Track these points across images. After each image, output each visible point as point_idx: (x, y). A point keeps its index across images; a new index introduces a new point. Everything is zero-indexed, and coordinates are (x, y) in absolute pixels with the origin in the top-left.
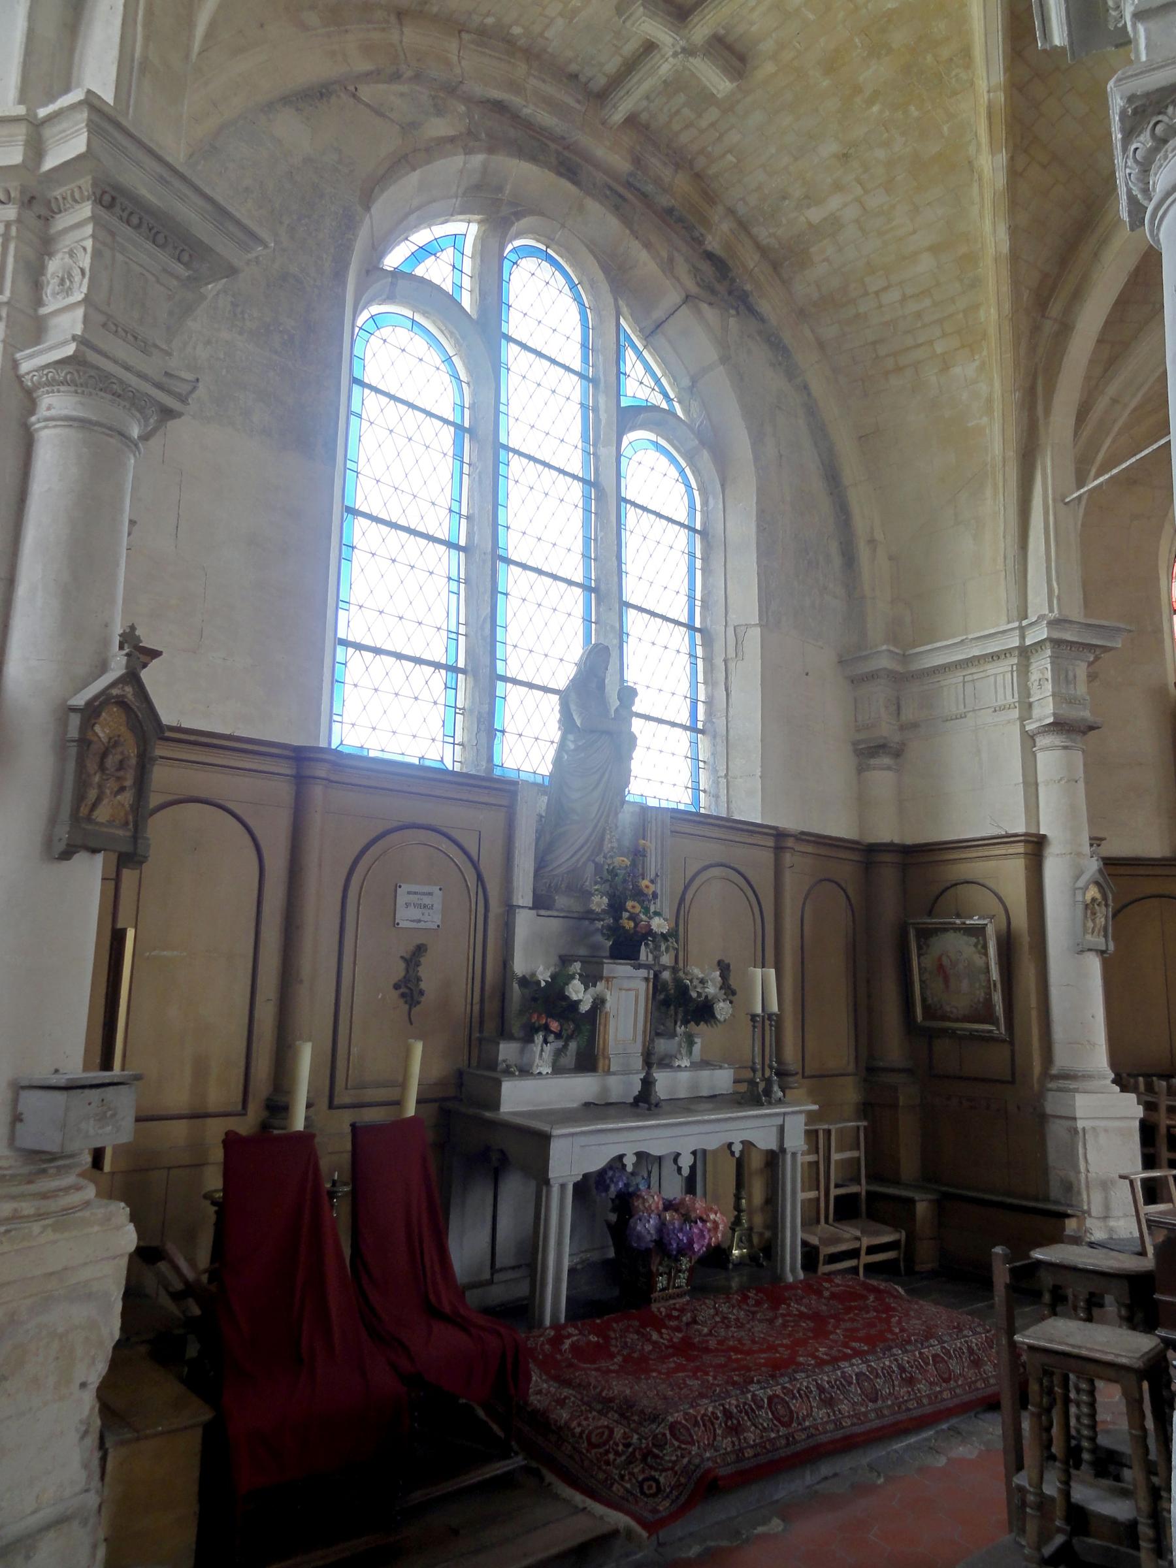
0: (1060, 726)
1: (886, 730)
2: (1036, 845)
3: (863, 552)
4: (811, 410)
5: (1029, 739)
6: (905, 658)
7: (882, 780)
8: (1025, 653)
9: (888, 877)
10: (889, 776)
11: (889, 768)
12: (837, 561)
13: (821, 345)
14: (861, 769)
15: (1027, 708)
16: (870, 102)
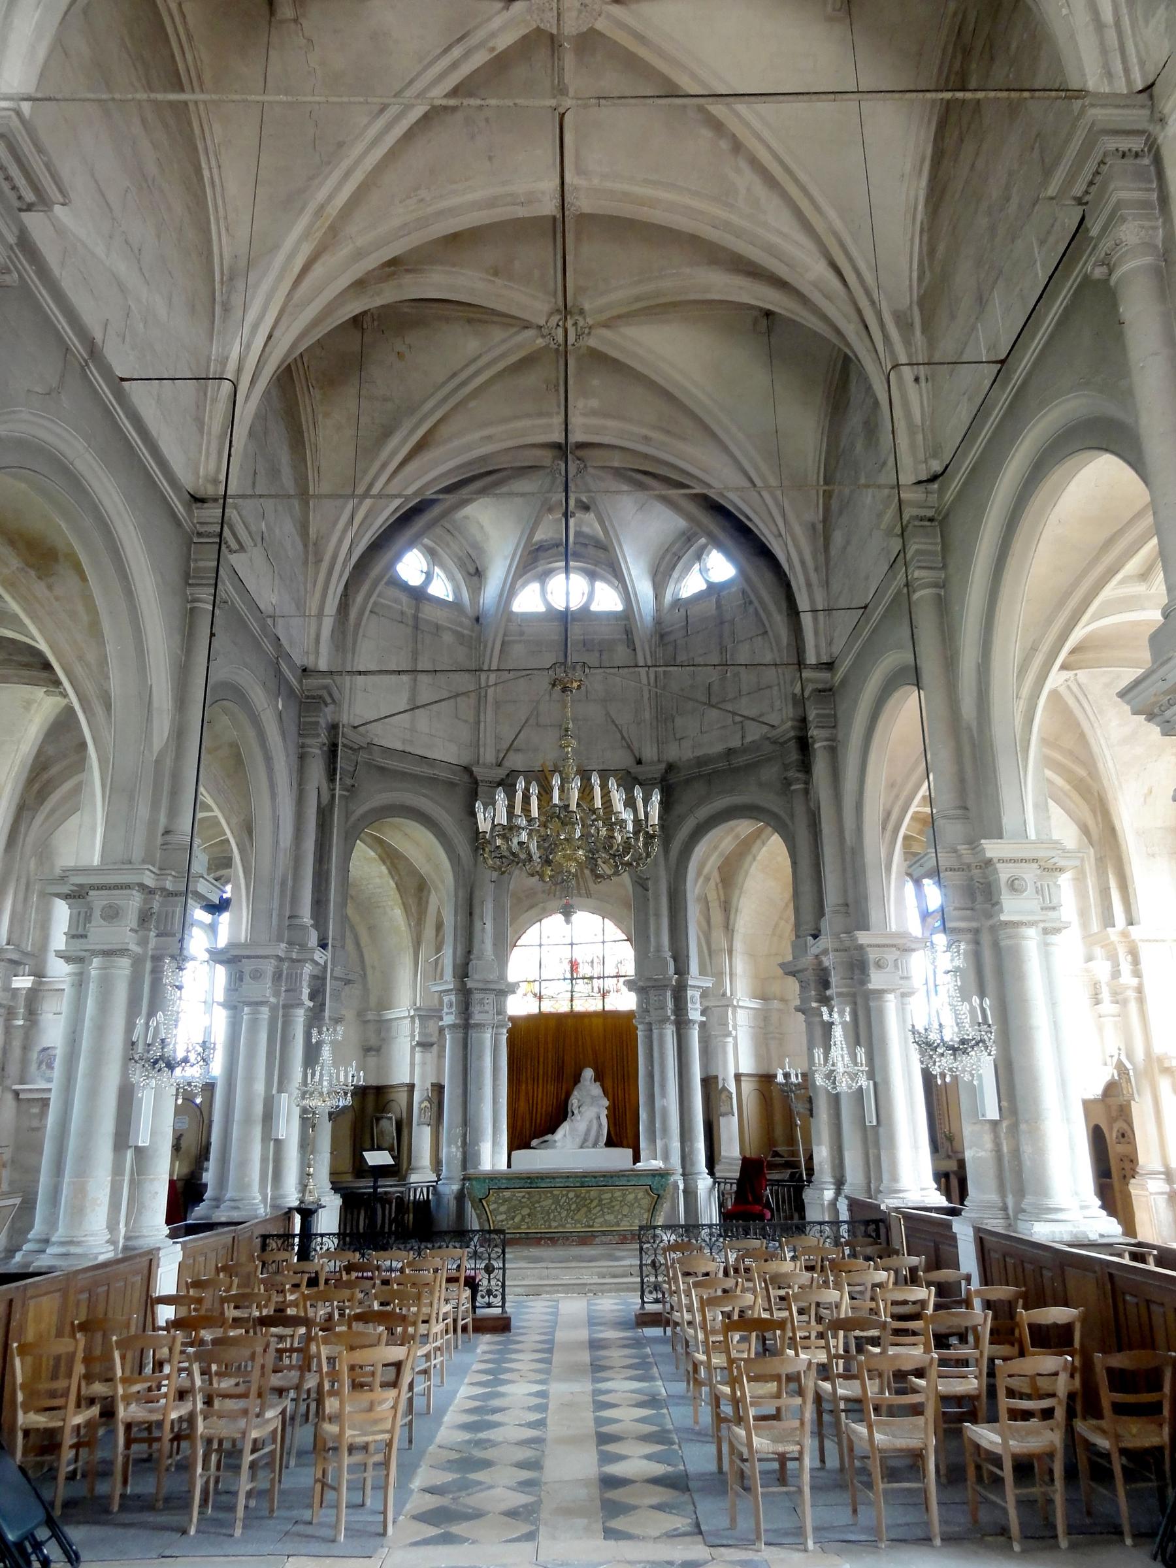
0: (419, 1044)
1: (373, 1042)
2: (411, 1087)
3: (369, 971)
5: (413, 1048)
6: (380, 1015)
7: (372, 1061)
9: (371, 1099)
10: (375, 1059)
15: (413, 1037)
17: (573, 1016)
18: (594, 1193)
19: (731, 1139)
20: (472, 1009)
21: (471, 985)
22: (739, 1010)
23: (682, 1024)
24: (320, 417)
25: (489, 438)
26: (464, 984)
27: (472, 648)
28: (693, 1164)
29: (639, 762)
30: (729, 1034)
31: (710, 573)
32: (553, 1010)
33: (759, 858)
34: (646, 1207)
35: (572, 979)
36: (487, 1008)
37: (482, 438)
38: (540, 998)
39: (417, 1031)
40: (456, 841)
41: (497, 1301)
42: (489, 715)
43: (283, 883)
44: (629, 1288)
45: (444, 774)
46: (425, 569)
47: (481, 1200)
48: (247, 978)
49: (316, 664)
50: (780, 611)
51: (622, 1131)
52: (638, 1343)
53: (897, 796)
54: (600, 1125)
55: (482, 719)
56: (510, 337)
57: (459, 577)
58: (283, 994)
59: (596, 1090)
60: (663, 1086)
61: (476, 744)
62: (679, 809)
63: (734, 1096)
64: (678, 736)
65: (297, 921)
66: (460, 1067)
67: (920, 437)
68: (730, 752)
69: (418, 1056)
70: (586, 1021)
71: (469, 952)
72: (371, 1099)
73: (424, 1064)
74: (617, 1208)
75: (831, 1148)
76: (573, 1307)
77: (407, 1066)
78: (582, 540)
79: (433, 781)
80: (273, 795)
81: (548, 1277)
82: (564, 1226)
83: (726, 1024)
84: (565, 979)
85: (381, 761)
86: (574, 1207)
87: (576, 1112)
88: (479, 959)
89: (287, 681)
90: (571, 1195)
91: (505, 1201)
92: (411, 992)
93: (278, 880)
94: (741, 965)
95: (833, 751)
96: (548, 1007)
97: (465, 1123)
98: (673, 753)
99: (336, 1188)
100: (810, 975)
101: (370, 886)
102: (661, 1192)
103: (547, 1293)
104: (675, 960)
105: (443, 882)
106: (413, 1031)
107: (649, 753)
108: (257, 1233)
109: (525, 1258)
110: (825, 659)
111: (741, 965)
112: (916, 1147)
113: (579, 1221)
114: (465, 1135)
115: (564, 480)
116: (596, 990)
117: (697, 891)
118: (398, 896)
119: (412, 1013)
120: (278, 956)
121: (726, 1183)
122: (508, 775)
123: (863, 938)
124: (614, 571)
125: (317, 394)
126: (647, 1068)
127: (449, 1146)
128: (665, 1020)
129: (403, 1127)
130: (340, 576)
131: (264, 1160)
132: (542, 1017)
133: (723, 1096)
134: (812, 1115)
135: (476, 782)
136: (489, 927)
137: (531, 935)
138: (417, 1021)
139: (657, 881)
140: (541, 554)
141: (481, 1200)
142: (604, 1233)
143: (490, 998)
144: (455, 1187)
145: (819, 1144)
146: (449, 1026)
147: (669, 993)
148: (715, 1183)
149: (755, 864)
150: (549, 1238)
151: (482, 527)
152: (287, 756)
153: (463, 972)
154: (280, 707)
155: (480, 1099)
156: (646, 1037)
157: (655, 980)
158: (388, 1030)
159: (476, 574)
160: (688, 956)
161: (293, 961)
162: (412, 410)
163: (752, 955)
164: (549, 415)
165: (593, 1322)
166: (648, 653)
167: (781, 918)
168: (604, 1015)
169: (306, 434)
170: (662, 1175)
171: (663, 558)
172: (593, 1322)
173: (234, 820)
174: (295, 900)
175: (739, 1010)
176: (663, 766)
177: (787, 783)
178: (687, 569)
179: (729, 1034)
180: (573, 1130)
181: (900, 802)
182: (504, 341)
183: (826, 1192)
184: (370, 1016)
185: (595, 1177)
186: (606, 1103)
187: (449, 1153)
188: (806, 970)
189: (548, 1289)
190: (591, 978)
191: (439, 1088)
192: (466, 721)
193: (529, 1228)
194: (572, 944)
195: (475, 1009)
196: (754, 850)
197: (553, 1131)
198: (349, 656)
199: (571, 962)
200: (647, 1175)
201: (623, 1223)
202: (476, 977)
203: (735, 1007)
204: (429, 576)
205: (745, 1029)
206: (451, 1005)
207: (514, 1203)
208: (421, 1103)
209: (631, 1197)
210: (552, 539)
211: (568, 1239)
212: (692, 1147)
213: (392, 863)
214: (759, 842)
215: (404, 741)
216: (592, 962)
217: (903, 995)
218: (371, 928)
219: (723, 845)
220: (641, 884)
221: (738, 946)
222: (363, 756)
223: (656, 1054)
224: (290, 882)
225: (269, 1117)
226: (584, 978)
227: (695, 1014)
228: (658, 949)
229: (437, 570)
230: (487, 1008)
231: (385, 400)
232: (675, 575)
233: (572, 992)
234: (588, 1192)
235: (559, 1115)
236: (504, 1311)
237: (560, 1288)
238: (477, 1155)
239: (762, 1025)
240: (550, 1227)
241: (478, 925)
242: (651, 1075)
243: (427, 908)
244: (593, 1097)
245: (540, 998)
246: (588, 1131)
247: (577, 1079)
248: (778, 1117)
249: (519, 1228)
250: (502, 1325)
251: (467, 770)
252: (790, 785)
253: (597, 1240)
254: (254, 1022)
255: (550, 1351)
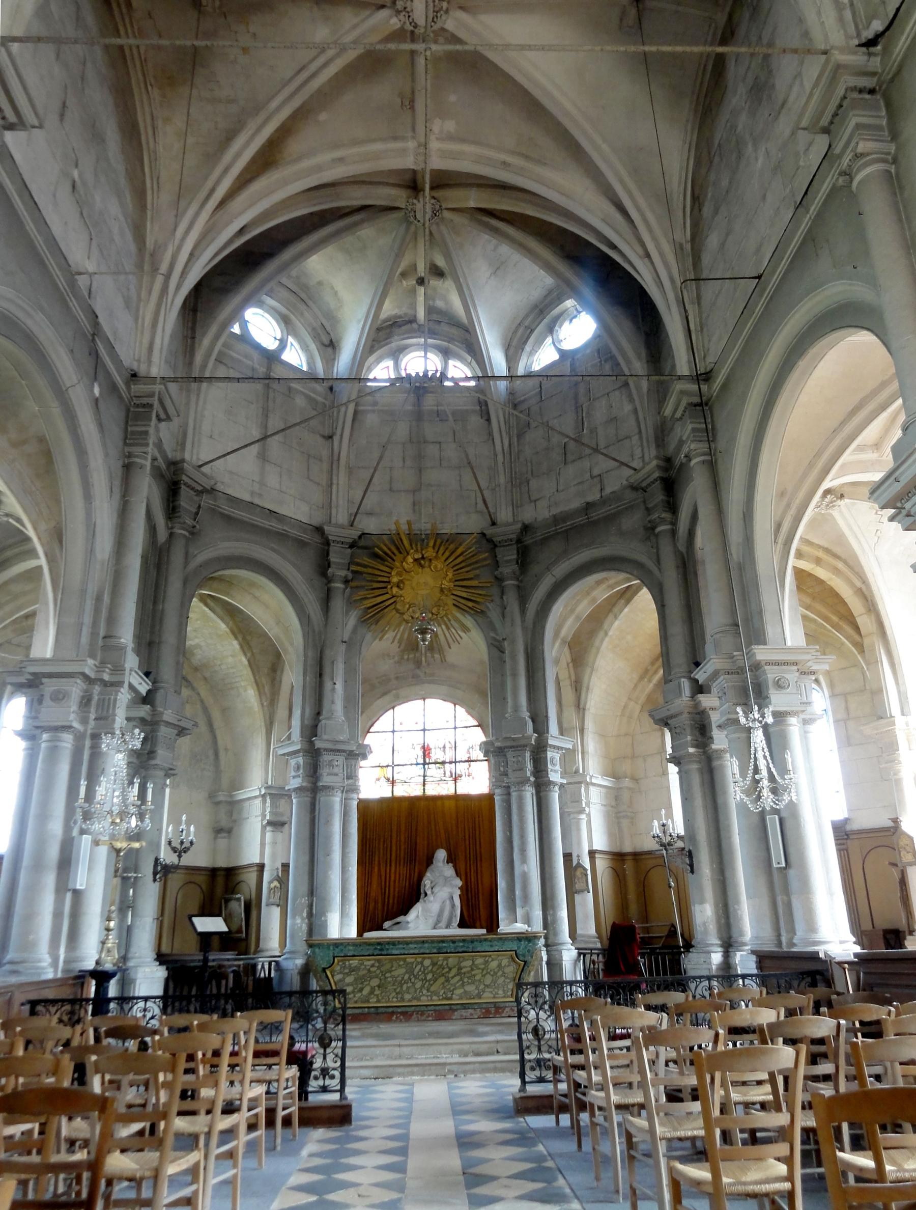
0: (270, 823)
1: (224, 823)
2: (261, 867)
3: (222, 753)
4: (202, 701)
5: (264, 828)
6: (231, 796)
7: (222, 842)
8: (264, 796)
9: (220, 881)
10: (225, 841)
11: (224, 838)
12: (212, 757)
13: (205, 679)
14: (215, 838)
15: (264, 816)
16: (197, 620)
17: (425, 799)
18: (452, 960)
19: (586, 917)
20: (320, 771)
21: (322, 755)
22: (591, 788)
23: (542, 785)
24: (160, 123)
25: (341, 160)
26: (312, 743)
27: (324, 408)
28: (556, 934)
29: (494, 524)
30: (582, 811)
31: (562, 344)
32: (406, 794)
33: (610, 633)
34: (511, 975)
35: (424, 764)
36: (336, 770)
37: (333, 160)
38: (393, 782)
39: (268, 810)
40: (306, 600)
41: (334, 1083)
42: (342, 478)
43: (99, 599)
44: (498, 1068)
45: (294, 532)
46: (279, 337)
47: (324, 970)
48: (47, 701)
49: (149, 372)
50: (639, 358)
51: (479, 907)
52: (523, 1138)
53: (788, 506)
54: (453, 906)
55: (335, 481)
56: (363, 21)
57: (313, 347)
58: (92, 723)
59: (449, 871)
60: (523, 851)
61: (328, 505)
62: (535, 569)
63: (589, 872)
64: (533, 498)
65: (112, 642)
66: (307, 834)
67: (848, 14)
68: (589, 506)
69: (268, 835)
70: (439, 803)
71: (319, 714)
72: (220, 881)
73: (274, 843)
74: (478, 977)
75: (716, 906)
76: (431, 1091)
77: (258, 845)
78: (435, 317)
79: (282, 537)
80: (88, 497)
81: (400, 1057)
82: (419, 1000)
83: (579, 801)
84: (417, 764)
85: (227, 509)
86: (429, 976)
87: (429, 892)
88: (328, 719)
89: (108, 374)
90: (427, 962)
91: (352, 970)
92: (264, 770)
93: (92, 589)
94: (592, 744)
95: (712, 466)
96: (401, 791)
97: (311, 892)
98: (528, 515)
99: (161, 958)
100: (685, 720)
101: (223, 667)
102: (528, 958)
103: (399, 1075)
104: (533, 721)
105: (292, 644)
106: (264, 810)
107: (504, 515)
108: (20, 997)
109: (377, 1036)
110: (701, 370)
111: (592, 744)
112: (831, 894)
113: (436, 993)
114: (311, 906)
115: (420, 210)
116: (448, 774)
117: (554, 653)
118: (250, 673)
119: (263, 792)
120: (84, 675)
121: (591, 954)
122: (360, 537)
123: (761, 654)
124: (466, 342)
125: (155, 93)
126: (504, 833)
127: (294, 917)
128: (524, 781)
129: (252, 908)
130: (178, 287)
131: (57, 915)
132: (394, 801)
133: (578, 873)
134: (692, 872)
135: (327, 543)
136: (339, 687)
137: (384, 722)
138: (268, 800)
139: (513, 642)
140: (396, 330)
141: (324, 970)
142: (464, 1006)
143: (340, 760)
144: (300, 962)
145: (702, 902)
146: (295, 790)
147: (528, 755)
148: (579, 954)
149: (607, 639)
150: (402, 1013)
151: (336, 293)
152: (107, 455)
153: (312, 730)
154: (96, 391)
155: (328, 866)
156: (503, 801)
157: (514, 740)
158: (240, 812)
159: (330, 346)
160: (547, 717)
161: (105, 684)
162: (257, 109)
163: (602, 736)
164: (403, 138)
165: (457, 1109)
166: (502, 419)
167: (629, 699)
168: (456, 798)
169: (143, 138)
170: (528, 938)
171: (515, 332)
172: (457, 1109)
173: (43, 526)
174: (112, 620)
175: (591, 788)
176: (519, 525)
177: (650, 529)
178: (540, 342)
179: (582, 811)
180: (425, 910)
181: (792, 511)
182: (355, 27)
183: (713, 955)
184: (221, 797)
185: (454, 942)
186: (459, 882)
187: (293, 925)
188: (681, 713)
189: (400, 1070)
190: (443, 763)
191: (286, 866)
192: (318, 484)
193: (378, 1001)
194: (424, 730)
195: (324, 772)
196: (605, 626)
197: (405, 912)
198: (193, 398)
199: (423, 747)
200: (512, 940)
201: (486, 995)
202: (325, 737)
203: (588, 784)
204: (283, 344)
205: (599, 807)
206: (298, 768)
207: (362, 973)
208: (270, 882)
209: (494, 964)
210: (406, 314)
211: (422, 1015)
212: (554, 915)
213: (244, 638)
214: (611, 616)
215: (252, 493)
216: (444, 747)
217: (806, 722)
218: (224, 711)
219: (580, 608)
220: (497, 647)
221: (590, 725)
222: (206, 501)
223: (515, 818)
224: (106, 598)
225: (66, 864)
226: (436, 763)
227: (555, 775)
228: (516, 709)
229: (290, 339)
230: (336, 770)
231: (231, 101)
232: (528, 348)
233: (424, 776)
234: (446, 959)
235: (411, 896)
236: (343, 1097)
237: (415, 1069)
238: (324, 926)
239: (613, 803)
240: (403, 1000)
241: (328, 685)
242: (509, 841)
243: (279, 689)
244: (446, 878)
245: (393, 782)
246: (440, 914)
247: (429, 861)
248: (632, 896)
249: (368, 1001)
250: (340, 1116)
251: (319, 530)
252: (653, 529)
253: (457, 1014)
254: (54, 751)
255: (403, 1151)
